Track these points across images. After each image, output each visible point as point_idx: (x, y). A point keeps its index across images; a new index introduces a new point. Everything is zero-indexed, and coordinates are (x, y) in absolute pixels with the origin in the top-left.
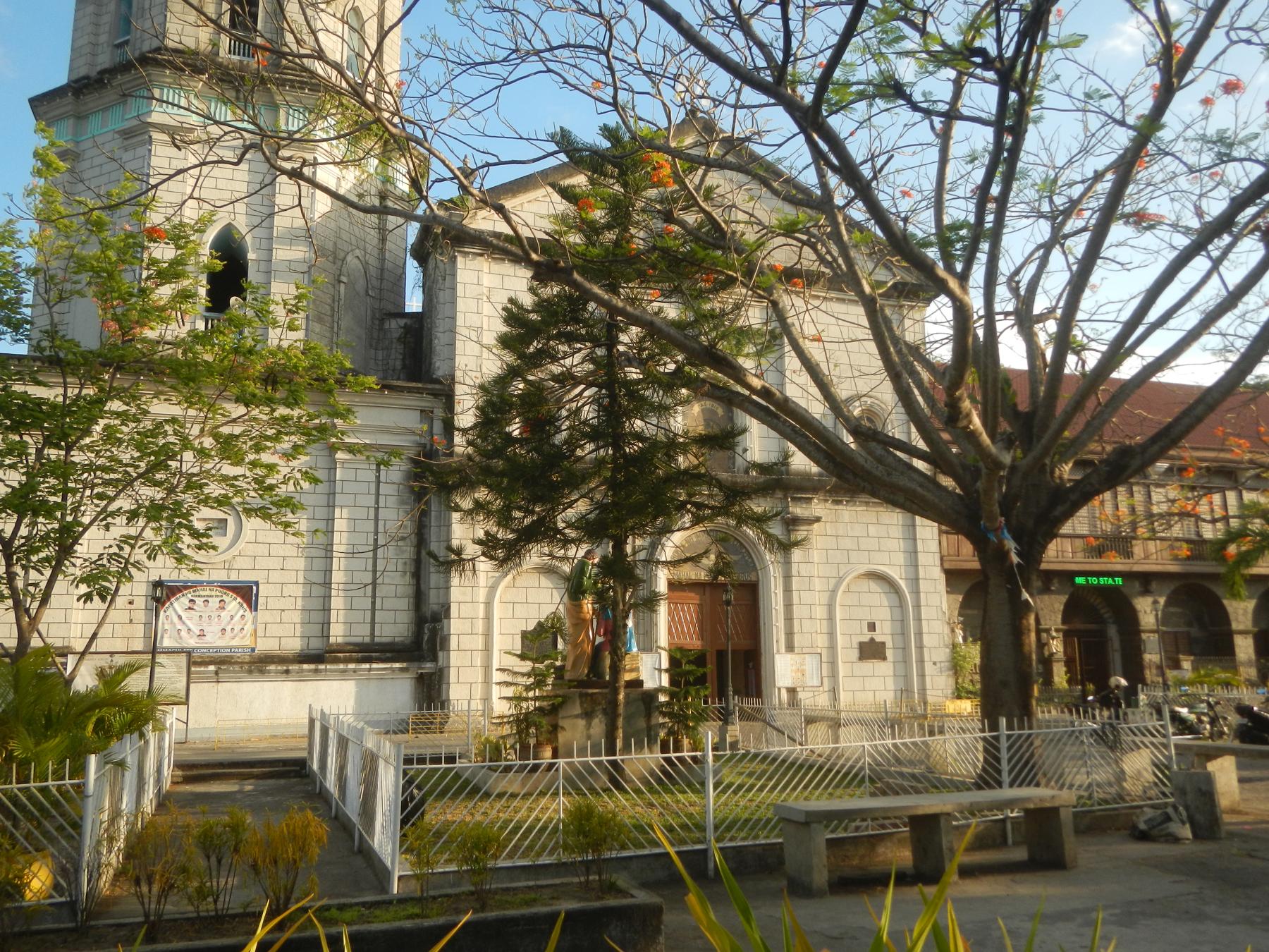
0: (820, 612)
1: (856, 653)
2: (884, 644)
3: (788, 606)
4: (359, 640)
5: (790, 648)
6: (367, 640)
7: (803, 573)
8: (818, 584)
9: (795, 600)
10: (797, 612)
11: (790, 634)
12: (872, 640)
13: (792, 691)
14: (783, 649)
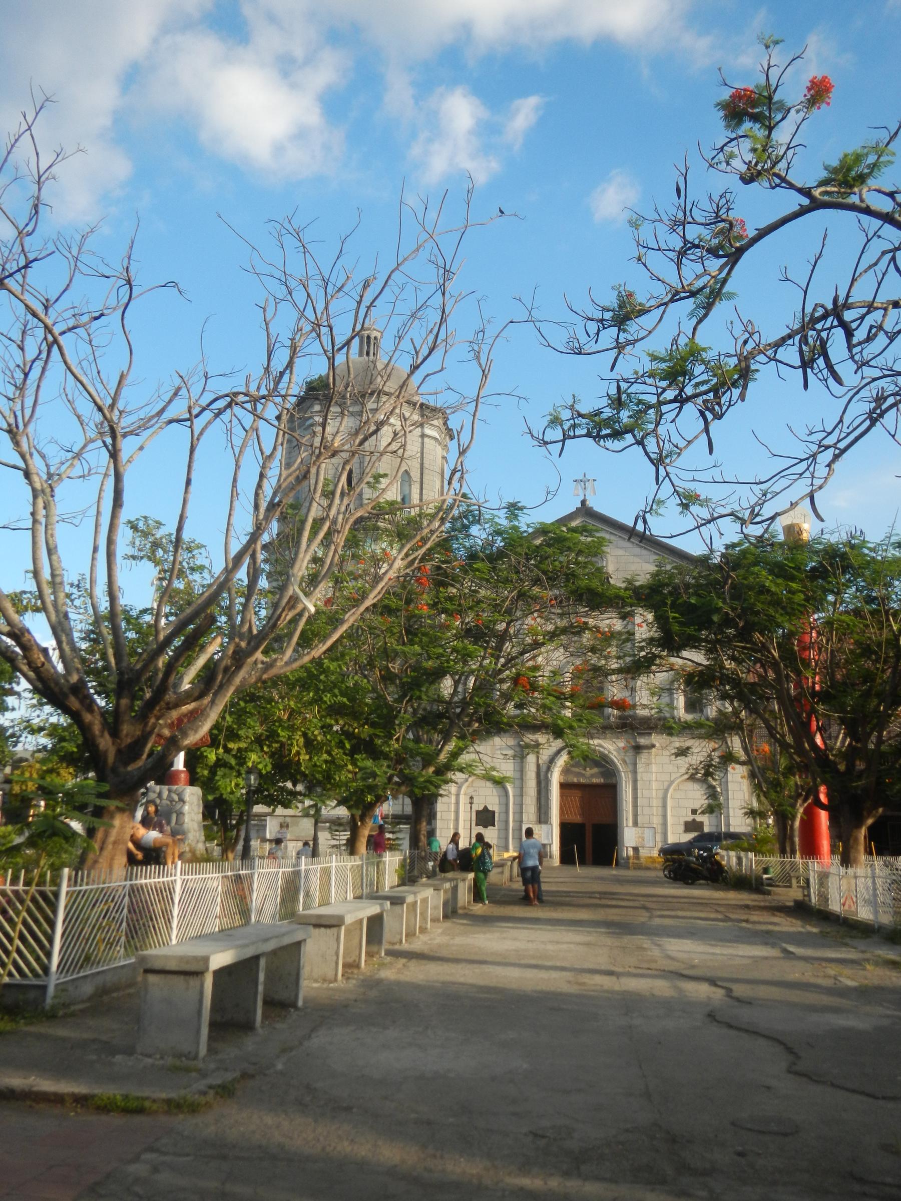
0: (657, 803)
1: (682, 828)
2: (702, 823)
3: (635, 798)
4: (396, 813)
5: (635, 824)
6: (400, 813)
7: (645, 778)
8: (654, 786)
9: (639, 795)
10: (640, 802)
11: (635, 816)
12: (694, 820)
13: (636, 849)
14: (630, 823)
